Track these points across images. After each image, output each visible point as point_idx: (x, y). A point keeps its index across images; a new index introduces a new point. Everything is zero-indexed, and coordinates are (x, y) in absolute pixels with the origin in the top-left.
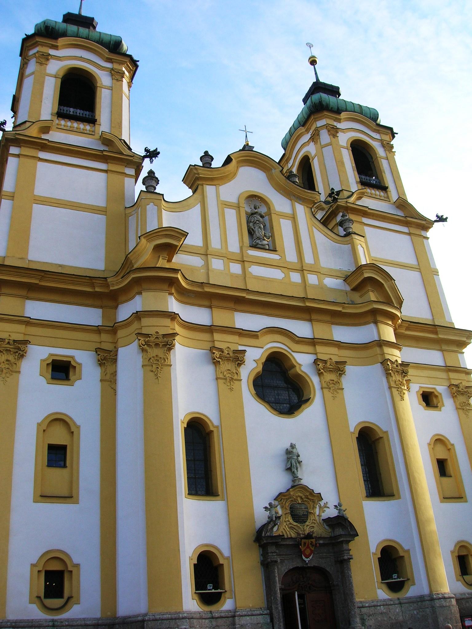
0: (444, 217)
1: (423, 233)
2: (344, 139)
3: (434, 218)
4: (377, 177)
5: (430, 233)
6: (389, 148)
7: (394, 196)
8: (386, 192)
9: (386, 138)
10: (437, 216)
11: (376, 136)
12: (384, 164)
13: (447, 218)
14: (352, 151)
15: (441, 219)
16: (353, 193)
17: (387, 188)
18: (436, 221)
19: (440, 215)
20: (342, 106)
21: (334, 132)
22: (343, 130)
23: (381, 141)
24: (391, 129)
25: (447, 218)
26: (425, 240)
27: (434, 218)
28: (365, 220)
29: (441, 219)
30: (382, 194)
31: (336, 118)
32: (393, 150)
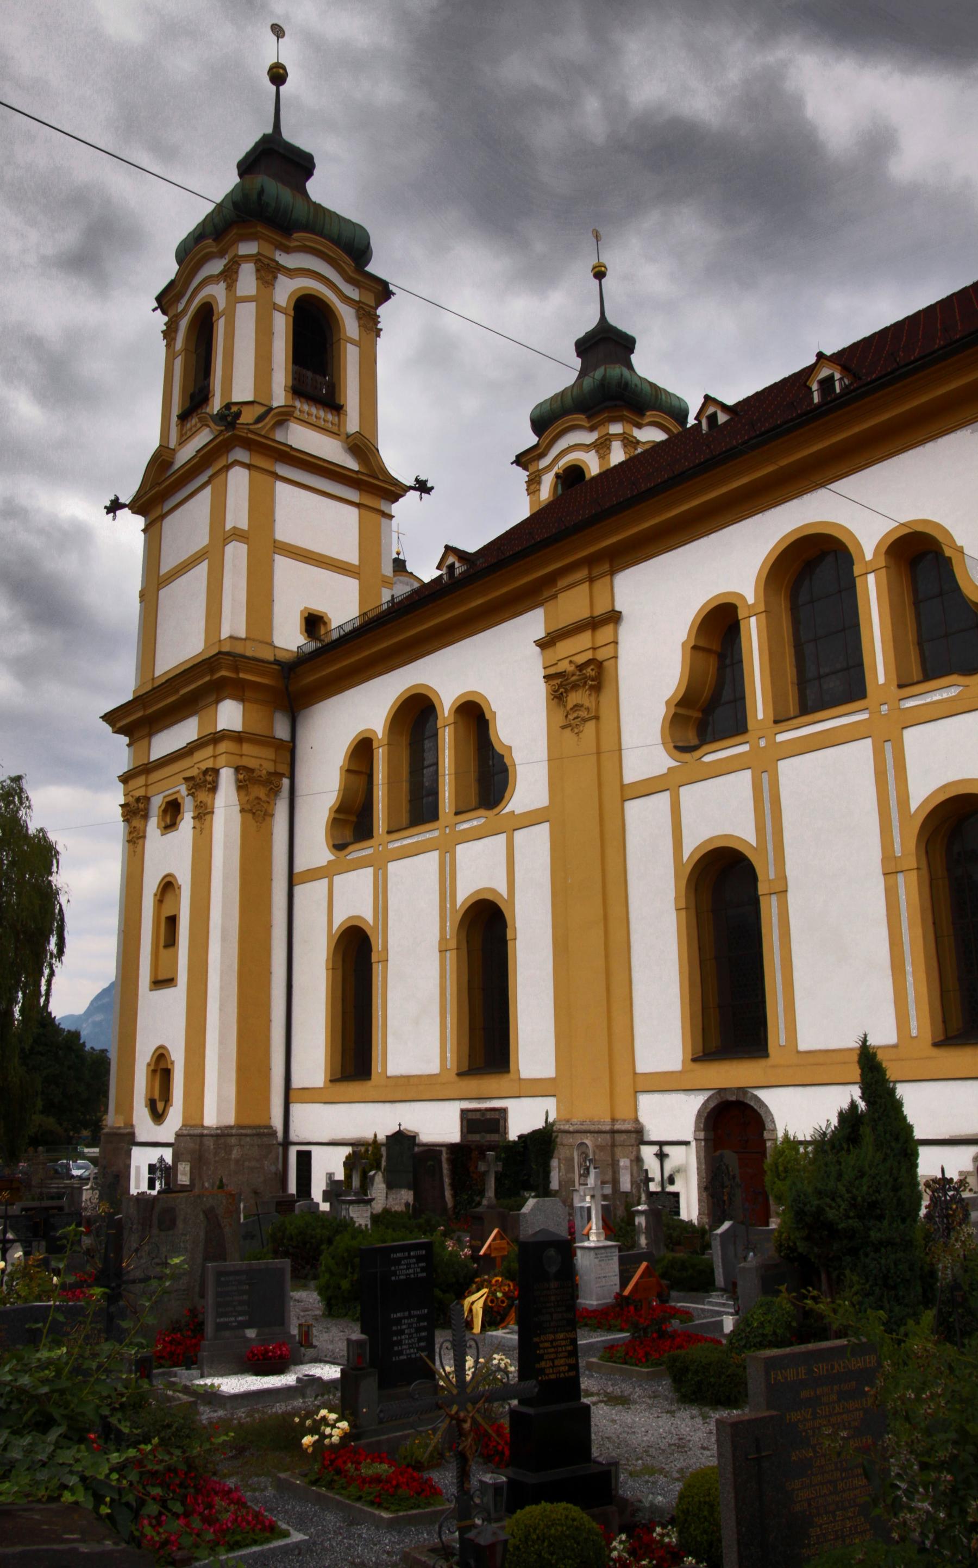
0: (429, 485)
1: (383, 506)
2: (285, 291)
3: (410, 482)
4: (332, 377)
5: (396, 508)
7: (352, 424)
8: (339, 415)
10: (417, 480)
12: (351, 357)
13: (432, 488)
15: (423, 487)
18: (411, 488)
19: (422, 478)
20: (300, 212)
21: (268, 271)
24: (385, 284)
25: (432, 488)
26: (384, 521)
27: (410, 482)
28: (282, 470)
29: (423, 487)
30: (330, 417)
31: (281, 244)
32: (379, 326)
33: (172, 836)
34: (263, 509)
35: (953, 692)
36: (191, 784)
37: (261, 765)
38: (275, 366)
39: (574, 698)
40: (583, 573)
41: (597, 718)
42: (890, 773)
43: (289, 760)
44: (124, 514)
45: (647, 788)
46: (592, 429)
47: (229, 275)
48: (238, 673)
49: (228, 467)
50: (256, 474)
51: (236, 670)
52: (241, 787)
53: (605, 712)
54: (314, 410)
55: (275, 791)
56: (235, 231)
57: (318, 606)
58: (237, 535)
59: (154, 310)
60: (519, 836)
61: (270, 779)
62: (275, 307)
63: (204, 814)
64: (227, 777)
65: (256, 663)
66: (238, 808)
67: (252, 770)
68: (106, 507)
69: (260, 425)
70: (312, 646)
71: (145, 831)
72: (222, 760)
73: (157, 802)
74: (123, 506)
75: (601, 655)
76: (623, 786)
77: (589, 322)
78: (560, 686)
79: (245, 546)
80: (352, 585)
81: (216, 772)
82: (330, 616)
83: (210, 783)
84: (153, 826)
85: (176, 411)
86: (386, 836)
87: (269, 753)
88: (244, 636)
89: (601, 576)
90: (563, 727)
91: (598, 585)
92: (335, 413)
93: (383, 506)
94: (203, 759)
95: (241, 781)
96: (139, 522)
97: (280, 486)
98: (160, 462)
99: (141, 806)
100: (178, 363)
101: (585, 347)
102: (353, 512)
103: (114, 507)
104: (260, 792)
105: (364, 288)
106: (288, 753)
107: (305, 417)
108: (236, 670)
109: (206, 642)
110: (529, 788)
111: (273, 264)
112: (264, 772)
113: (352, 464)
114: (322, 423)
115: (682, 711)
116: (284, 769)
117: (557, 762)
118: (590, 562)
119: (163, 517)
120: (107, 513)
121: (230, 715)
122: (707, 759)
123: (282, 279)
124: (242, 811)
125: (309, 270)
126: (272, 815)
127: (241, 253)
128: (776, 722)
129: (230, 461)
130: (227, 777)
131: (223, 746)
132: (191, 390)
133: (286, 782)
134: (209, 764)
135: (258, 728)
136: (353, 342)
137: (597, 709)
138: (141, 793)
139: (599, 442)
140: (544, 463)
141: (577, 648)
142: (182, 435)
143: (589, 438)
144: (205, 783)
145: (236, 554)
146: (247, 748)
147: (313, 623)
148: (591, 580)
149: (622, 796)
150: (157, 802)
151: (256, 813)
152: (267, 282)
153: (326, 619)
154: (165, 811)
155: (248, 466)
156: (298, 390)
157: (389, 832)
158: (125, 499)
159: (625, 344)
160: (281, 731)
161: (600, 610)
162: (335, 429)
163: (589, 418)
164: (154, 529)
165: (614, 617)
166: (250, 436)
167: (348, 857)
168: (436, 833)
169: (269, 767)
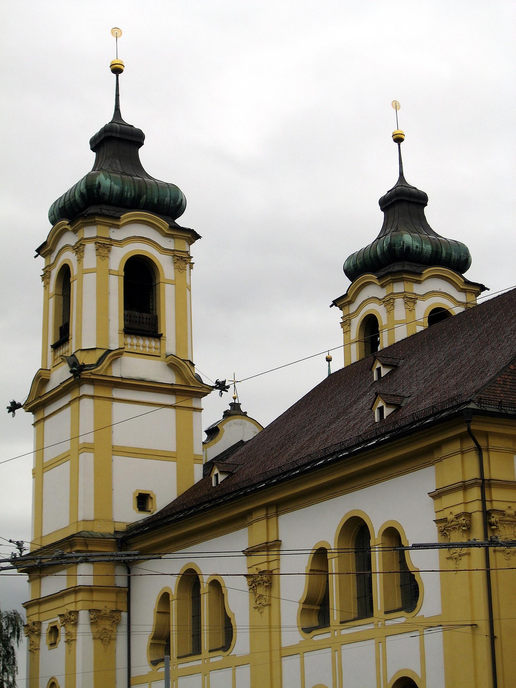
6: (183, 260)
7: (170, 345)
8: (160, 340)
9: (182, 245)
11: (168, 244)
14: (125, 278)
16: (109, 351)
17: (161, 335)
18: (213, 387)
19: (220, 380)
21: (104, 246)
22: (120, 243)
23: (173, 253)
26: (195, 414)
28: (117, 393)
30: (153, 343)
31: (113, 224)
33: (54, 651)
34: (104, 427)
35: (403, 620)
36: (63, 619)
37: (106, 607)
38: (111, 317)
39: (260, 590)
40: (262, 514)
41: (270, 605)
42: (381, 660)
43: (126, 599)
44: (20, 412)
45: (294, 651)
46: (383, 286)
47: (78, 249)
48: (87, 547)
49: (80, 398)
50: (98, 402)
51: (87, 545)
52: (93, 623)
53: (274, 602)
54: (141, 342)
55: (116, 623)
56: (80, 222)
57: (144, 488)
58: (87, 448)
59: (36, 257)
60: (238, 670)
61: (112, 618)
62: (110, 272)
63: (70, 641)
64: (84, 617)
65: (102, 538)
66: (92, 637)
67: (100, 611)
68: (8, 408)
69: (99, 368)
70: (142, 516)
71: (39, 645)
72: (80, 606)
73: (45, 627)
74: (19, 406)
75: (273, 566)
76: (281, 649)
77: (390, 183)
78: (253, 582)
79: (92, 454)
80: (171, 466)
81: (77, 612)
82: (155, 492)
83: (73, 621)
84: (44, 641)
85: (51, 342)
86: (176, 660)
87: (112, 597)
88: (92, 518)
89: (272, 517)
90: (255, 608)
91: (273, 520)
92: (157, 340)
93: (195, 405)
94: (69, 604)
95: (92, 620)
96: (30, 417)
97: (116, 405)
98: (41, 380)
99: (36, 628)
100: (52, 301)
101: (388, 203)
102: (172, 412)
103: (14, 407)
104: (106, 624)
105: (177, 238)
106: (127, 592)
107: (135, 349)
108: (87, 545)
109: (70, 521)
110: (242, 643)
111: (107, 242)
112: (108, 610)
113: (169, 378)
114: (147, 350)
115: (307, 607)
116: (123, 606)
117: (253, 628)
118: (267, 506)
119: (44, 419)
120: (9, 412)
121: (85, 574)
122: (316, 638)
123: (115, 249)
124: (94, 638)
125: (135, 237)
126: (115, 639)
127: (86, 236)
128: (341, 623)
129: (81, 394)
130: (84, 617)
131: (81, 596)
132: (61, 325)
133: (124, 615)
134: (72, 608)
135: (104, 582)
136: (169, 282)
137: (270, 600)
138: (35, 619)
139: (387, 298)
140: (353, 308)
141: (260, 560)
142: (55, 360)
143: (381, 293)
144: (71, 619)
145: (87, 460)
146: (96, 596)
147: (143, 500)
148: (267, 518)
149: (280, 654)
150: (45, 627)
151: (104, 639)
152: (103, 256)
153: (151, 496)
154: (50, 632)
155: (92, 397)
156: (129, 330)
157: (178, 658)
158: (21, 399)
159: (419, 200)
160: (121, 582)
161: (272, 538)
162: (157, 353)
163: (379, 278)
164: (40, 425)
165: (278, 543)
166: (92, 377)
167: (159, 671)
168: (200, 662)
169: (113, 607)
